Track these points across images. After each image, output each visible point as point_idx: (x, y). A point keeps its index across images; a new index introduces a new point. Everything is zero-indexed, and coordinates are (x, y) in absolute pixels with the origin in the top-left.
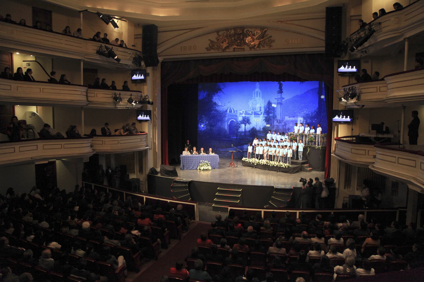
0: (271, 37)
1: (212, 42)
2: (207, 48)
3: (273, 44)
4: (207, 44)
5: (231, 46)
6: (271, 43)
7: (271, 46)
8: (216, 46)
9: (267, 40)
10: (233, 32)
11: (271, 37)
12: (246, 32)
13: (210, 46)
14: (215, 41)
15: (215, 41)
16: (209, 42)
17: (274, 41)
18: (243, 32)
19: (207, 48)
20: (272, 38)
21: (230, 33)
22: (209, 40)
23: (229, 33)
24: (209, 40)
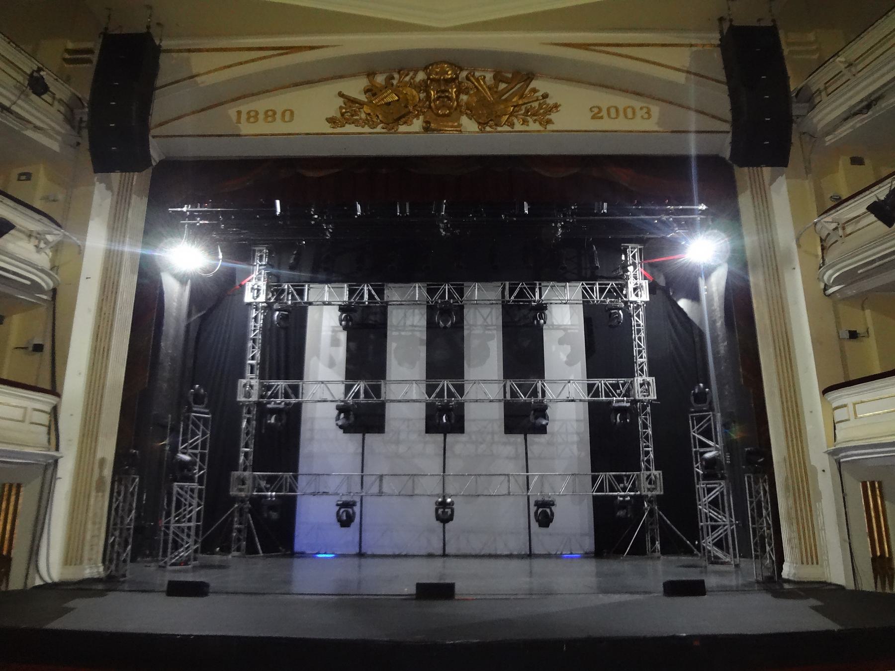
0: (545, 96)
1: (350, 101)
2: (332, 121)
3: (553, 116)
4: (333, 107)
5: (417, 116)
6: (545, 113)
7: (549, 122)
8: (363, 116)
9: (536, 105)
10: (421, 76)
11: (545, 96)
12: (467, 78)
13: (342, 114)
14: (363, 98)
15: (363, 98)
16: (340, 102)
17: (556, 106)
18: (457, 78)
19: (332, 121)
20: (550, 101)
21: (412, 78)
22: (341, 95)
23: (407, 79)
24: (341, 95)
